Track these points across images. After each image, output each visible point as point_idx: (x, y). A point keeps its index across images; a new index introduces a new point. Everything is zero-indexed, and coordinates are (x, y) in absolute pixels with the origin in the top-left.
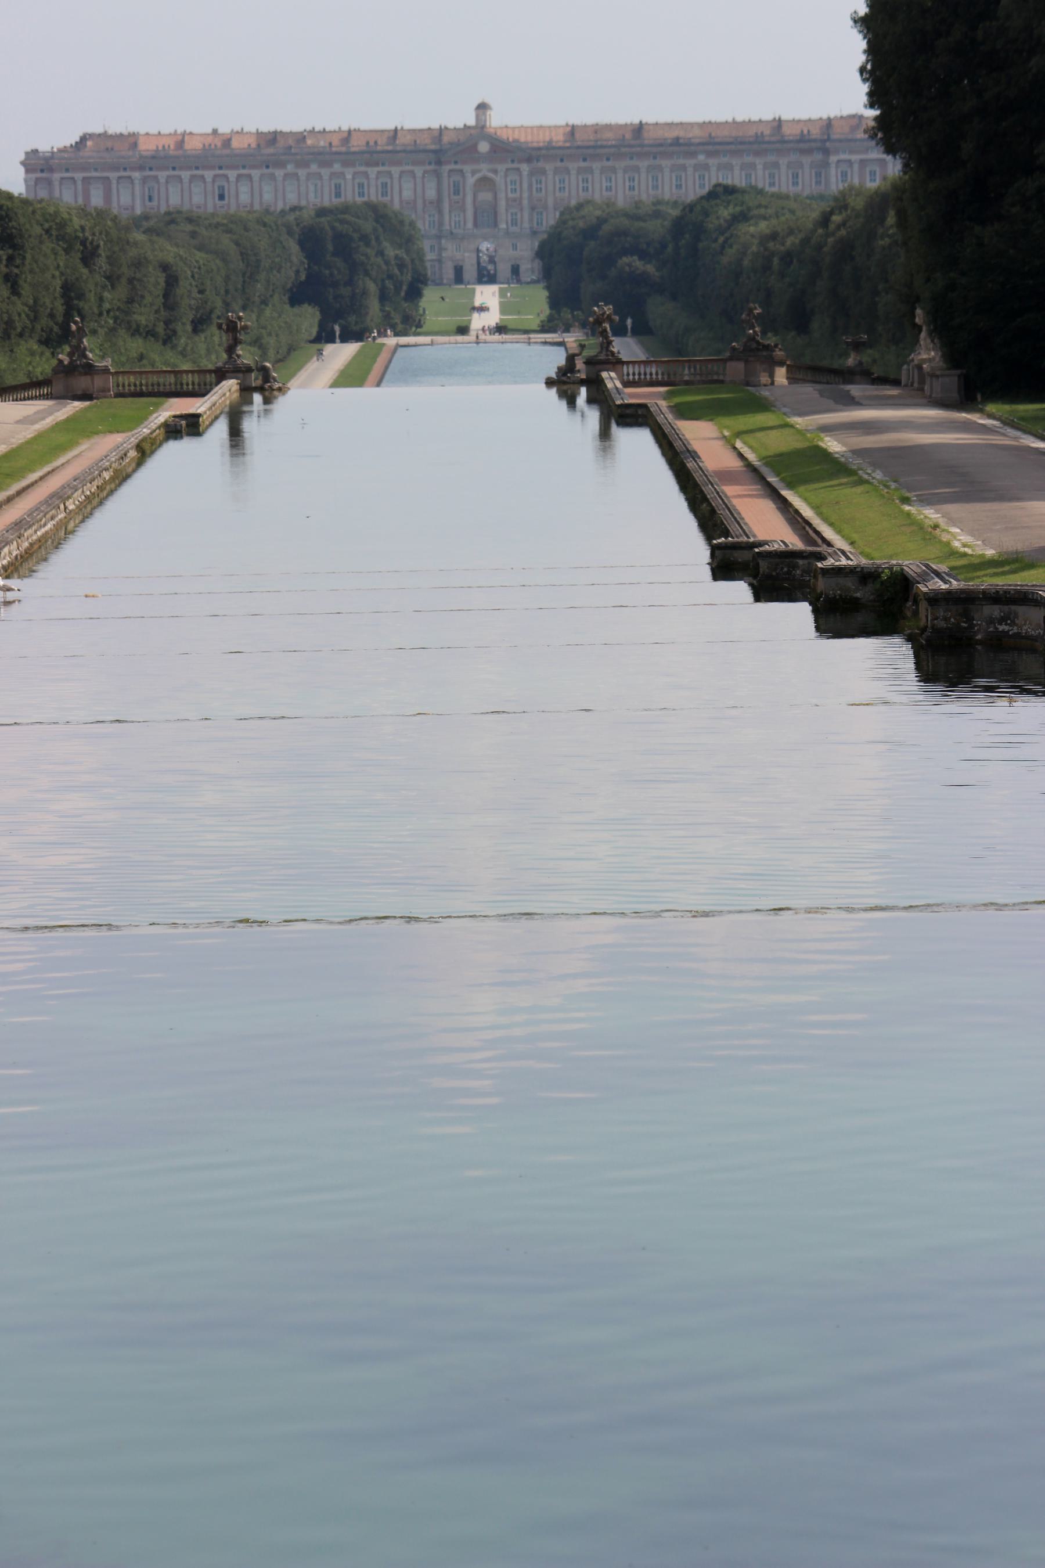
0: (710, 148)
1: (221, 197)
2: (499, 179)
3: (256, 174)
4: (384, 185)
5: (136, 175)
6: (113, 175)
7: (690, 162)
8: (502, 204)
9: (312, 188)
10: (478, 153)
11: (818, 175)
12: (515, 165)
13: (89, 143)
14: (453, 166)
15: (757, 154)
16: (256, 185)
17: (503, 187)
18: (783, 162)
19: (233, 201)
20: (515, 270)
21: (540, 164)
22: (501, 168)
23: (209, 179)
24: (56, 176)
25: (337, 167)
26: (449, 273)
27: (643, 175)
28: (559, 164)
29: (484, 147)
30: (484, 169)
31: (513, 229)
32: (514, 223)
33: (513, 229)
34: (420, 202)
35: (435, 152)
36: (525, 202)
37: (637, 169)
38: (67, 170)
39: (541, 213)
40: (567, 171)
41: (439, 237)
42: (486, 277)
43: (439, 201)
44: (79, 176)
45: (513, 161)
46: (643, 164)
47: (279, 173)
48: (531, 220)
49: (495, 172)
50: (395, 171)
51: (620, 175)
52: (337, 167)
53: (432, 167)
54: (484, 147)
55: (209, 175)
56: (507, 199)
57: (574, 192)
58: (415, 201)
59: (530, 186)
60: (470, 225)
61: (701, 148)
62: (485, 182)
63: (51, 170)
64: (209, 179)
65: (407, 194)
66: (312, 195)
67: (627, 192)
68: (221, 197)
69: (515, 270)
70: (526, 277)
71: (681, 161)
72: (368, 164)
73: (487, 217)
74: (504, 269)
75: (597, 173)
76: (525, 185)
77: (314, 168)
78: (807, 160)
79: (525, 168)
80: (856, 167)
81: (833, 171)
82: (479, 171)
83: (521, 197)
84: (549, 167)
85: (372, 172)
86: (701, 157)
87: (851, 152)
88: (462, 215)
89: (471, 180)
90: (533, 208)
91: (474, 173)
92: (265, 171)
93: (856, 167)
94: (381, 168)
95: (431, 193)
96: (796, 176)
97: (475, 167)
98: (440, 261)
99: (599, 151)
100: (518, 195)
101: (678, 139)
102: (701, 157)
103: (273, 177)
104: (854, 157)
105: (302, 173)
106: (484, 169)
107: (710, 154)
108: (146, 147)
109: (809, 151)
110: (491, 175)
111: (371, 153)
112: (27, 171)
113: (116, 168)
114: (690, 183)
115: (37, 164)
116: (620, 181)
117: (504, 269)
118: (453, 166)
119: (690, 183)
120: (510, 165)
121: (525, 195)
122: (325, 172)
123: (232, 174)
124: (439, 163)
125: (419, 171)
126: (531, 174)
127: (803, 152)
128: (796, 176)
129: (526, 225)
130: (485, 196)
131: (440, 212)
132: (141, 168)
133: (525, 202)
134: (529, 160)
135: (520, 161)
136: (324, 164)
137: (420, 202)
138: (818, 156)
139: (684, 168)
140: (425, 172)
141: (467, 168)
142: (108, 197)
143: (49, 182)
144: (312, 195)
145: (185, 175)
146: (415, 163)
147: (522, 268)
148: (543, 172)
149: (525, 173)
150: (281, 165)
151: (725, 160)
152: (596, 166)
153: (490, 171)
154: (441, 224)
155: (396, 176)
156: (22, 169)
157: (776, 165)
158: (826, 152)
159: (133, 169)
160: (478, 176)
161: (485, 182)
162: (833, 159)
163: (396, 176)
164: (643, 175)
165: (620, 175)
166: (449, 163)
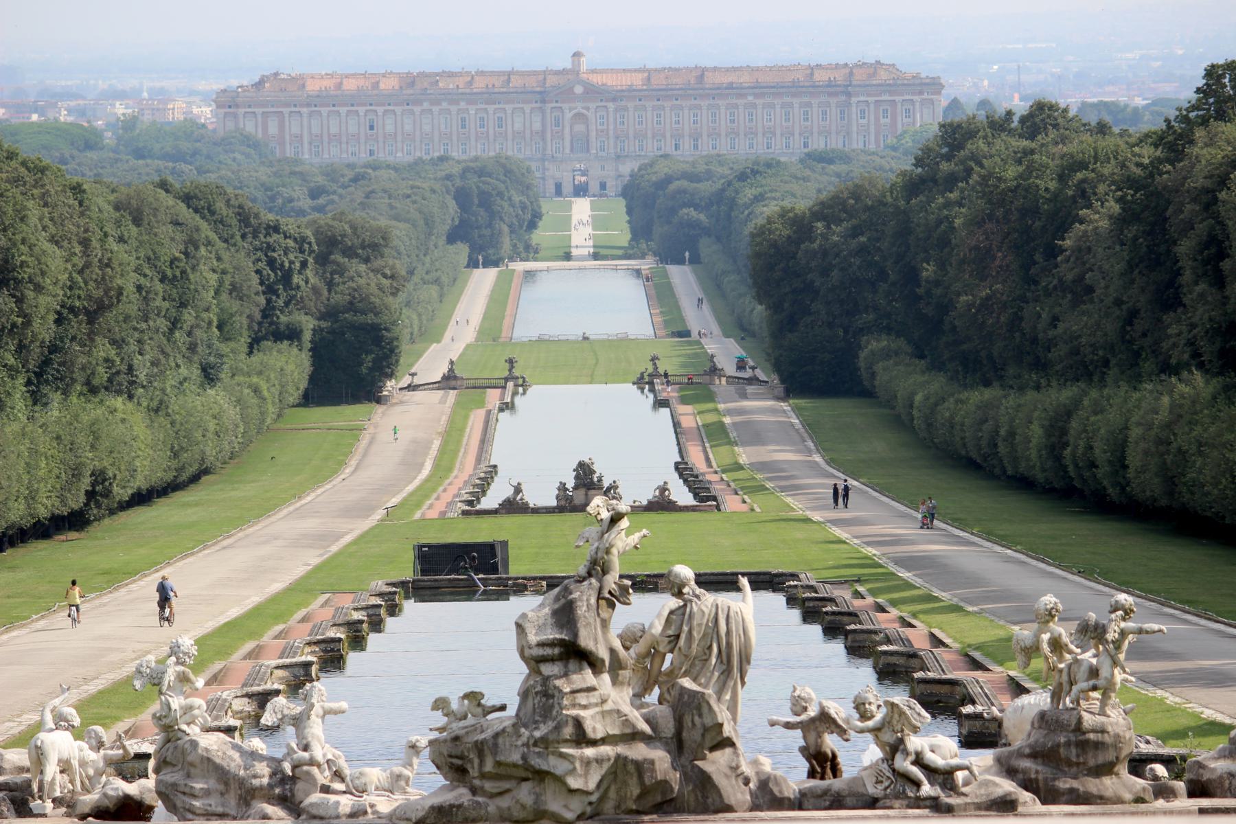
0: (757, 91)
1: (372, 128)
2: (590, 114)
3: (398, 110)
4: (500, 119)
5: (305, 110)
6: (286, 110)
7: (741, 102)
8: (593, 134)
11: (842, 112)
13: (267, 85)
14: (554, 105)
15: (794, 95)
16: (399, 118)
18: (815, 102)
19: (381, 131)
20: (603, 186)
21: (623, 103)
22: (592, 106)
23: (361, 114)
24: (241, 111)
25: (463, 105)
26: (551, 188)
27: (704, 112)
28: (638, 103)
29: (579, 90)
30: (579, 107)
31: (601, 154)
32: (602, 149)
33: (601, 154)
34: (528, 132)
35: (540, 93)
38: (250, 106)
40: (644, 108)
41: (543, 160)
42: (581, 191)
43: (544, 131)
44: (259, 111)
46: (704, 103)
47: (417, 109)
48: (616, 147)
49: (588, 109)
50: (509, 108)
51: (686, 111)
52: (463, 105)
53: (538, 105)
54: (579, 90)
55: (362, 110)
59: (616, 119)
60: (567, 151)
61: (751, 91)
62: (579, 116)
63: (237, 106)
64: (361, 114)
65: (518, 126)
66: (443, 126)
68: (372, 128)
69: (603, 186)
70: (611, 191)
71: (735, 101)
72: (487, 103)
73: (582, 144)
74: (594, 187)
75: (667, 109)
76: (611, 120)
77: (445, 105)
78: (833, 101)
79: (611, 106)
80: (872, 106)
81: (854, 109)
84: (630, 105)
85: (491, 108)
86: (750, 98)
87: (869, 95)
89: (568, 115)
90: (617, 138)
92: (407, 107)
93: (872, 106)
94: (497, 106)
95: (537, 126)
96: (824, 113)
97: (573, 105)
98: (543, 179)
99: (670, 93)
101: (731, 83)
102: (750, 98)
103: (412, 112)
104: (871, 99)
105: (436, 109)
106: (579, 107)
107: (756, 96)
108: (312, 87)
109: (835, 94)
110: (585, 111)
111: (490, 94)
112: (218, 107)
113: (287, 105)
114: (741, 118)
115: (228, 102)
117: (594, 187)
118: (554, 105)
119: (741, 118)
121: (611, 127)
122: (454, 108)
123: (380, 110)
124: (544, 101)
125: (527, 108)
126: (616, 110)
127: (830, 94)
128: (824, 113)
129: (612, 150)
130: (579, 128)
131: (544, 140)
132: (308, 105)
133: (611, 133)
134: (614, 100)
136: (452, 102)
137: (528, 132)
138: (843, 98)
139: (736, 106)
140: (532, 109)
141: (565, 106)
143: (235, 116)
144: (443, 126)
145: (343, 110)
146: (525, 102)
147: (608, 185)
148: (626, 109)
150: (418, 102)
151: (768, 100)
152: (667, 104)
154: (545, 149)
155: (509, 112)
157: (809, 104)
158: (849, 95)
159: (302, 105)
160: (574, 112)
161: (579, 116)
162: (854, 100)
163: (509, 112)
164: (704, 112)
165: (686, 111)
166: (551, 102)
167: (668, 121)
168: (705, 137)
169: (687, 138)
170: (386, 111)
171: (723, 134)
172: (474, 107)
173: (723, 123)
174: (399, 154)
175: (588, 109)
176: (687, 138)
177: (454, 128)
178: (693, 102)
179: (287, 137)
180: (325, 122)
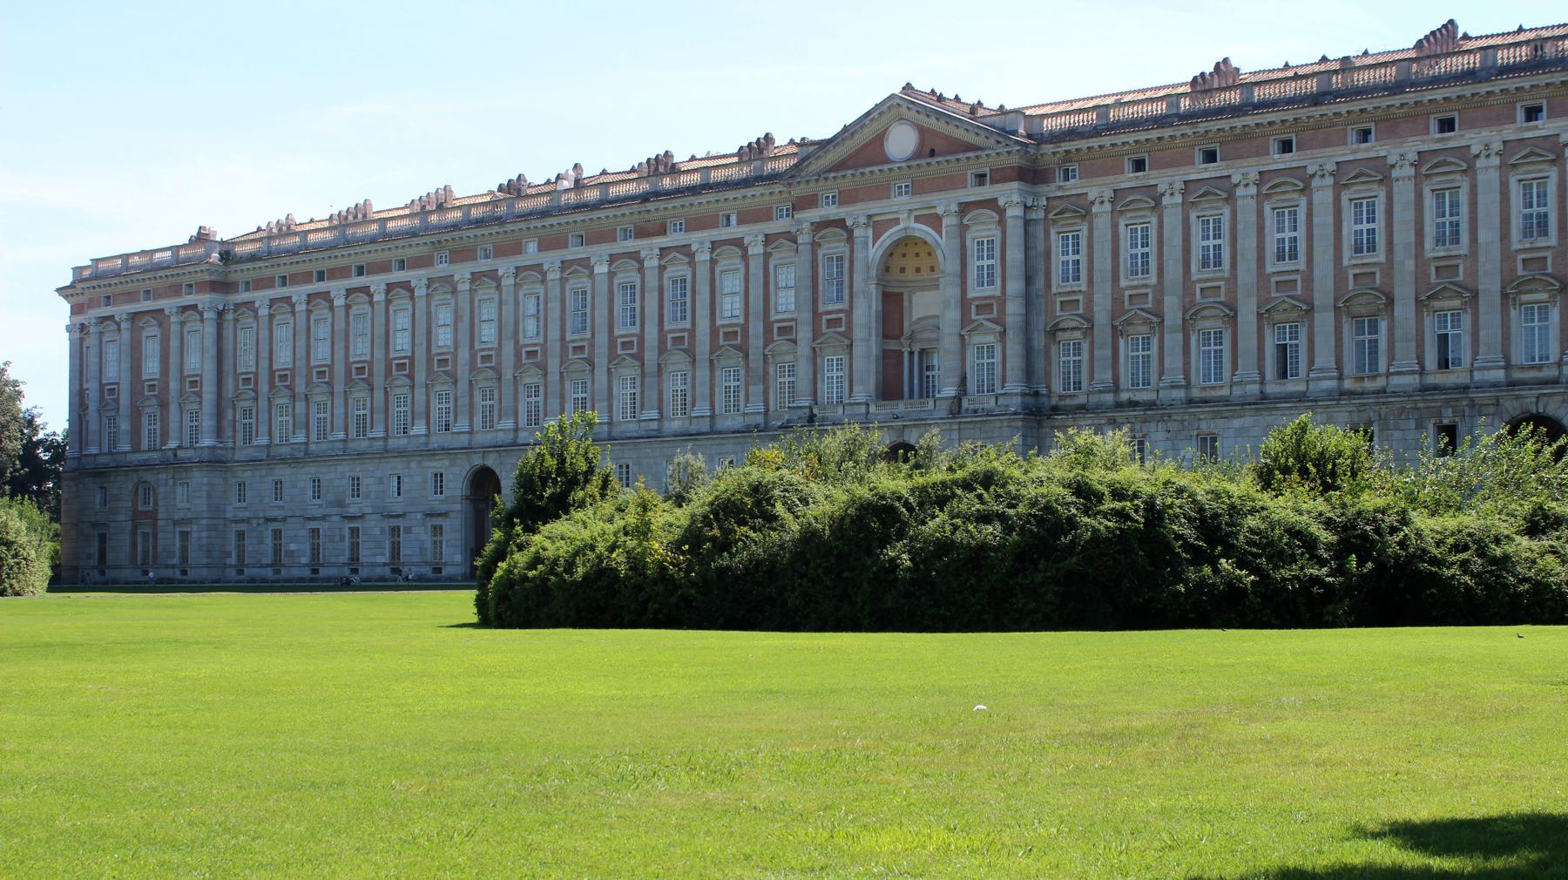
9: (530, 307)
10: (887, 160)
12: (987, 192)
17: (952, 266)
21: (1074, 186)
22: (945, 203)
27: (1404, 192)
28: (1201, 171)
34: (756, 328)
36: (1014, 309)
37: (1382, 172)
39: (1078, 350)
45: (981, 179)
49: (934, 221)
50: (699, 240)
51: (1323, 196)
56: (964, 303)
57: (1173, 271)
58: (745, 328)
66: (530, 326)
67: (1347, 253)
79: (1010, 194)
83: (1002, 300)
84: (1097, 190)
85: (649, 248)
91: (879, 227)
97: (874, 207)
100: (994, 290)
106: (902, 211)
110: (923, 230)
116: (1323, 219)
120: (973, 194)
134: (1032, 174)
135: (1000, 176)
141: (855, 214)
144: (530, 326)
149: (1014, 212)
156: (65, 307)
164: (1404, 192)
165: (1323, 196)
167: (1248, 243)
168: (1404, 310)
169: (1324, 321)
170: (390, 287)
171: (1490, 286)
172: (606, 249)
173: (1488, 235)
174: (419, 429)
176: (1324, 321)
177: (554, 334)
178: (1351, 151)
179: (174, 385)
180: (264, 334)
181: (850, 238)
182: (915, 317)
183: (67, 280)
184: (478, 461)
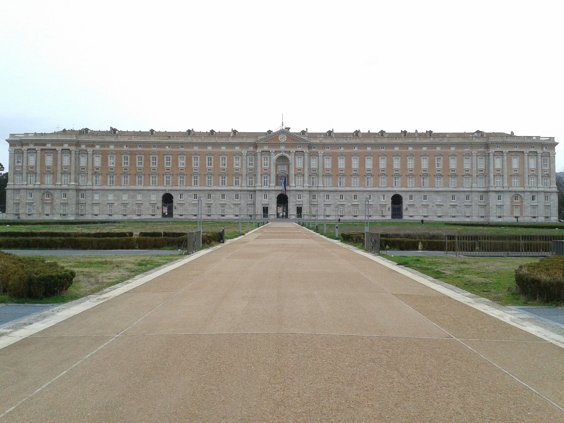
2: (291, 158)
6: (59, 148)
8: (292, 172)
22: (293, 150)
26: (260, 211)
49: (289, 153)
62: (283, 159)
69: (299, 210)
82: (280, 152)
88: (268, 177)
89: (274, 158)
91: (276, 152)
130: (282, 169)
141: (272, 150)
142: (55, 160)
153: (285, 152)
156: (8, 144)
175: (289, 153)
181: (270, 155)
182: (279, 170)
183: (8, 137)
184: (166, 192)
